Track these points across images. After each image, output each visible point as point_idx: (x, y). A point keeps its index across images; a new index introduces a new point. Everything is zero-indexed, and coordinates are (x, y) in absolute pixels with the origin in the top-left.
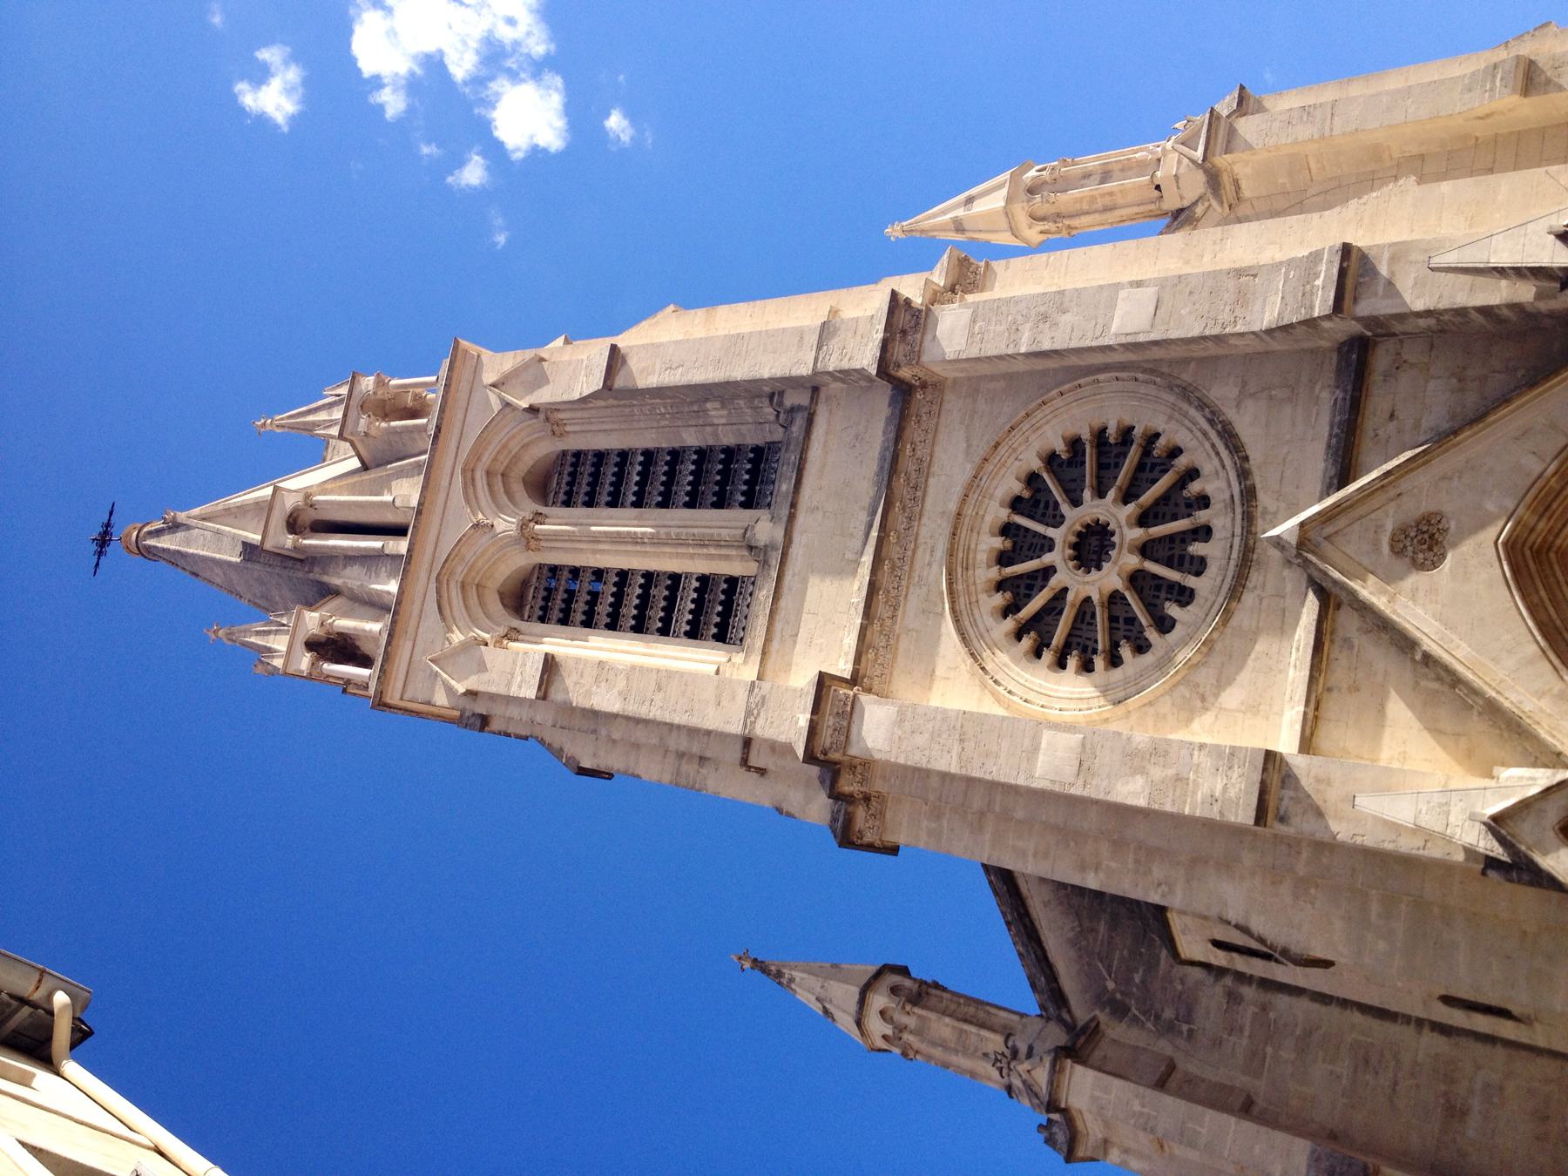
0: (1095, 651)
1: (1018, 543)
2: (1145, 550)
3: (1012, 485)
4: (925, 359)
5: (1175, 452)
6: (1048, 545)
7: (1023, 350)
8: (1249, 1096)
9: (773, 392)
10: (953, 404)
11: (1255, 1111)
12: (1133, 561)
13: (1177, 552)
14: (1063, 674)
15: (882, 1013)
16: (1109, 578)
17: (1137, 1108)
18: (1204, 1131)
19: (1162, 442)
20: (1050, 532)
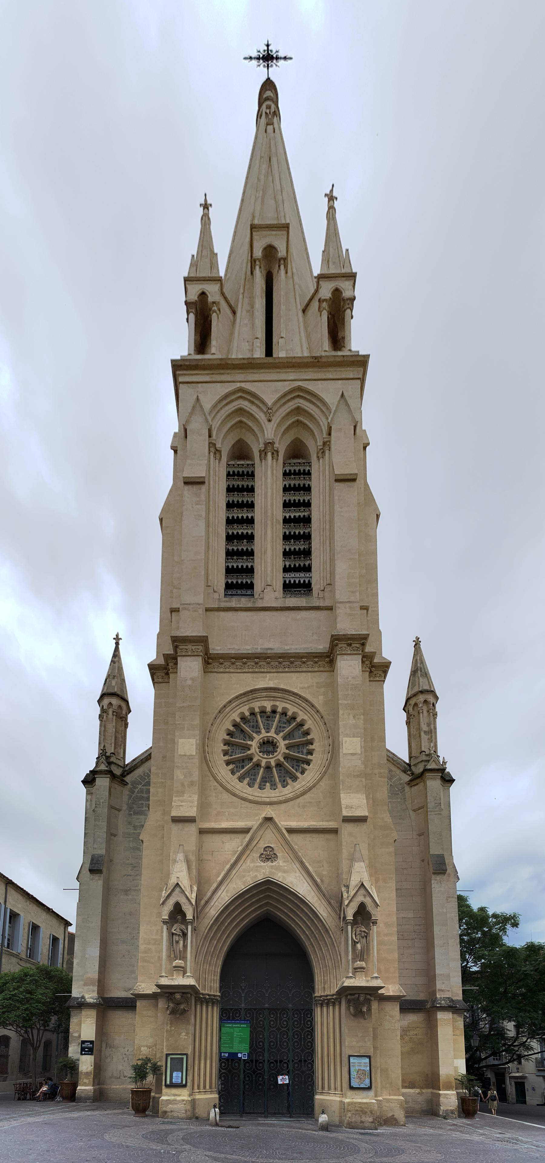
0: (231, 756)
2: (268, 768)
3: (291, 710)
6: (268, 730)
10: (322, 678)
13: (268, 780)
14: (222, 745)
16: (258, 757)
19: (305, 766)
20: (273, 730)
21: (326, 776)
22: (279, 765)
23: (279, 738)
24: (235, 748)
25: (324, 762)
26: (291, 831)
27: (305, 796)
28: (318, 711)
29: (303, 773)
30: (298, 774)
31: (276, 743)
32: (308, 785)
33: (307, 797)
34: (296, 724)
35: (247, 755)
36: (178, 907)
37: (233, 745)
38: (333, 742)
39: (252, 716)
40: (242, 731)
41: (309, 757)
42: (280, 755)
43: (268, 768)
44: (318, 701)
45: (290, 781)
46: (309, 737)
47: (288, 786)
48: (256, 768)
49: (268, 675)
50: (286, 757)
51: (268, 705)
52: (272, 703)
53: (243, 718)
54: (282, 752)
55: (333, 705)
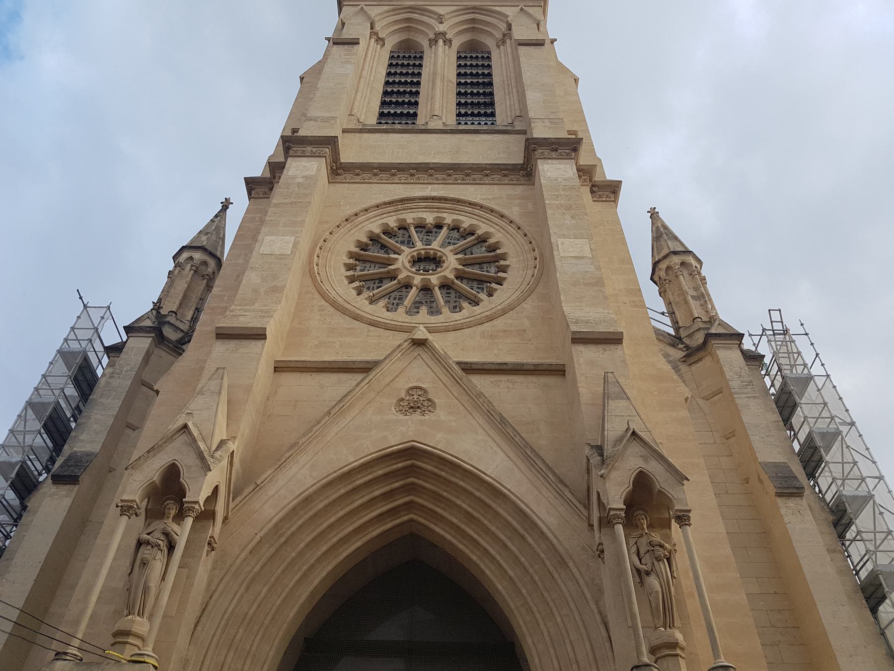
1: (428, 230)
2: (426, 289)
3: (466, 222)
4: (539, 161)
5: (490, 295)
7: (547, 202)
8: (138, 428)
9: (523, 115)
10: (519, 190)
11: (129, 431)
12: (417, 280)
15: (191, 258)
17: (125, 369)
18: (109, 401)
19: (494, 285)
21: (533, 296)
22: (446, 286)
23: (447, 251)
24: (368, 265)
25: (527, 279)
26: (469, 369)
27: (495, 322)
28: (511, 222)
29: (490, 295)
30: (483, 296)
31: (441, 257)
32: (499, 307)
33: (499, 323)
34: (477, 239)
35: (388, 272)
36: (172, 473)
37: (365, 261)
38: (542, 255)
39: (401, 231)
40: (383, 246)
41: (501, 274)
42: (448, 271)
43: (426, 289)
44: (514, 212)
45: (465, 304)
46: (498, 251)
47: (464, 311)
48: (404, 290)
49: (430, 187)
50: (460, 276)
51: (430, 218)
52: (435, 215)
53: (387, 232)
54: (450, 268)
55: (539, 215)
